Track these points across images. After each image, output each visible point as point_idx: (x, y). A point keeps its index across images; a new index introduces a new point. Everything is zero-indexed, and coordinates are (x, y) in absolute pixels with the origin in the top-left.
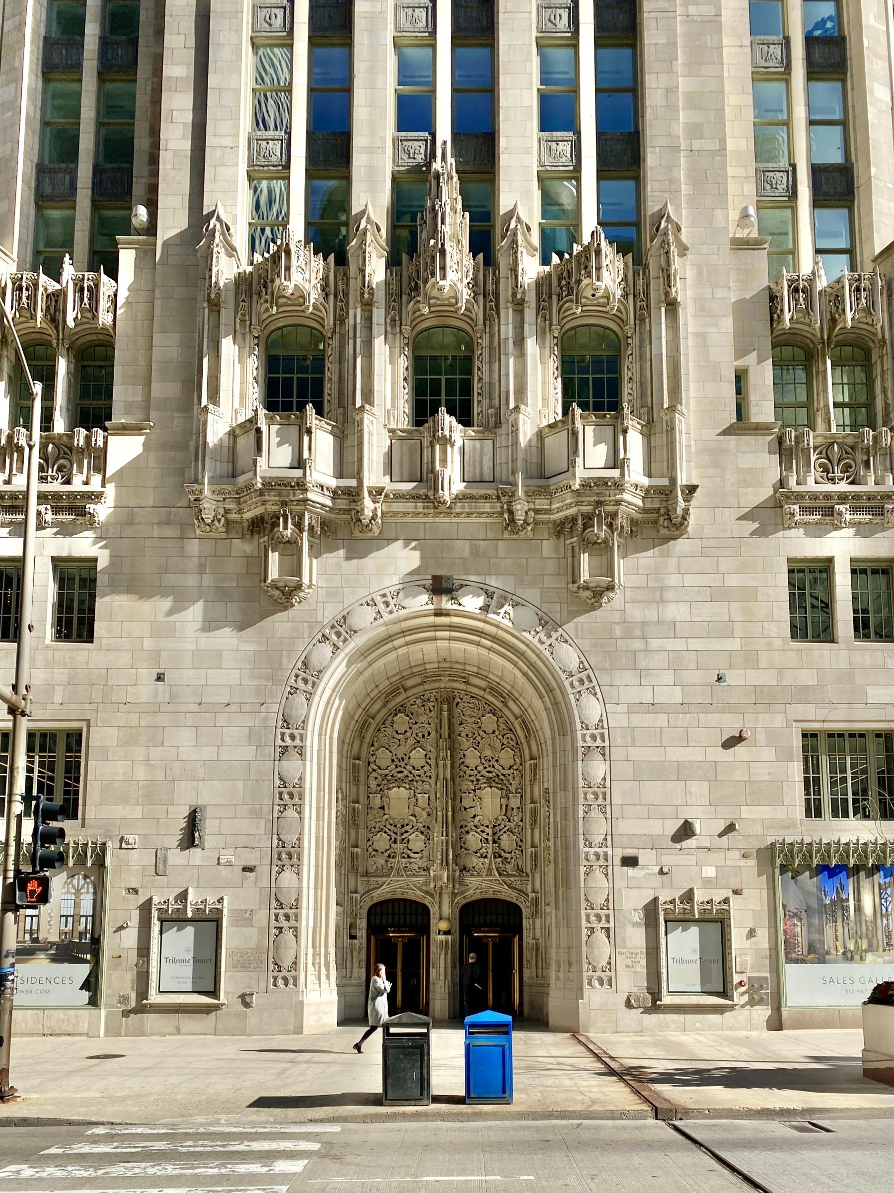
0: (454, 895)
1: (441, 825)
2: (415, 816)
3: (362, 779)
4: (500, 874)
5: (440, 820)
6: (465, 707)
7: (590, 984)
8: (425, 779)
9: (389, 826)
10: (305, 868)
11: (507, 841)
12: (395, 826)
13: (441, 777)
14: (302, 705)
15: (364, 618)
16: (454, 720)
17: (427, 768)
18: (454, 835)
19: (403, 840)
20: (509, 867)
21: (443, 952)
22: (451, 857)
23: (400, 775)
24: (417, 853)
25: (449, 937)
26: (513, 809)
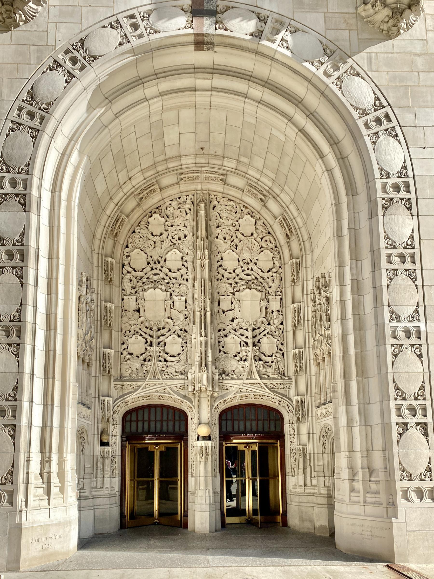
0: (213, 399)
1: (199, 326)
2: (172, 319)
3: (116, 279)
4: (261, 378)
5: (198, 320)
6: (224, 213)
7: (405, 496)
8: (181, 282)
9: (144, 330)
10: (28, 348)
11: (268, 345)
12: (151, 329)
13: (199, 277)
14: (27, 144)
15: (106, 42)
16: (211, 223)
17: (183, 271)
18: (213, 336)
19: (159, 343)
20: (270, 371)
21: (203, 459)
22: (210, 359)
23: (155, 277)
24: (174, 356)
25: (209, 443)
26: (273, 312)
